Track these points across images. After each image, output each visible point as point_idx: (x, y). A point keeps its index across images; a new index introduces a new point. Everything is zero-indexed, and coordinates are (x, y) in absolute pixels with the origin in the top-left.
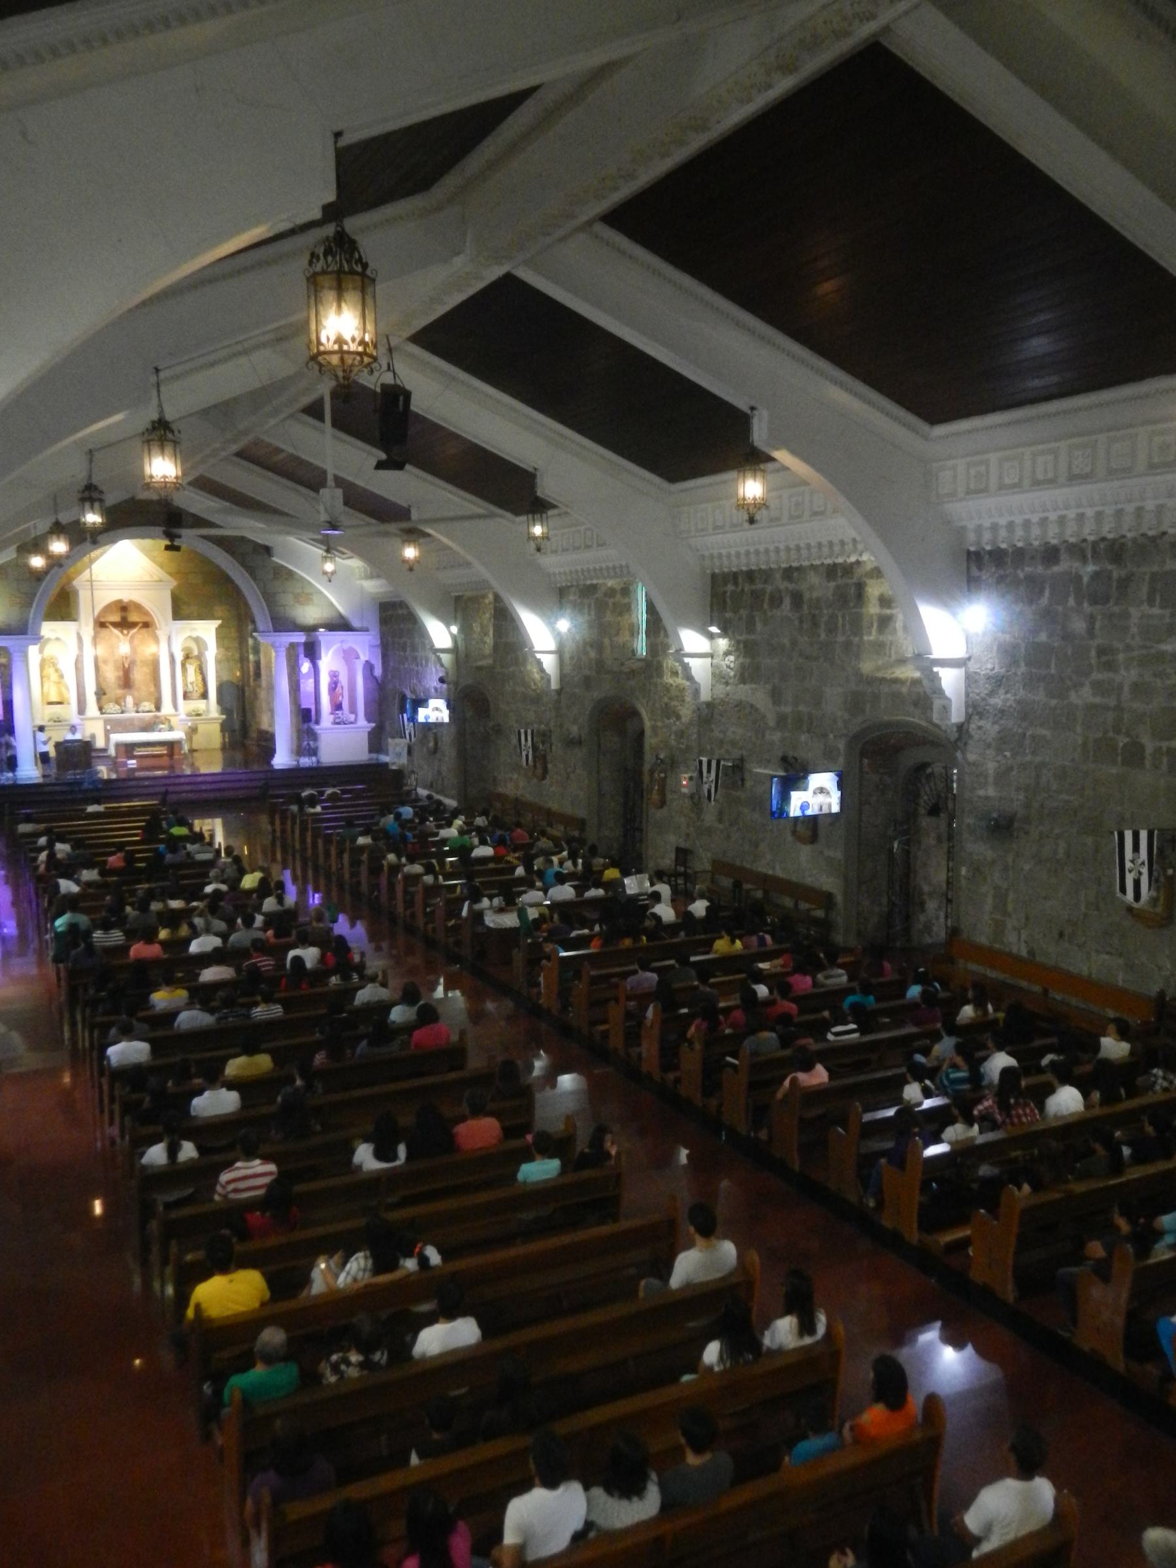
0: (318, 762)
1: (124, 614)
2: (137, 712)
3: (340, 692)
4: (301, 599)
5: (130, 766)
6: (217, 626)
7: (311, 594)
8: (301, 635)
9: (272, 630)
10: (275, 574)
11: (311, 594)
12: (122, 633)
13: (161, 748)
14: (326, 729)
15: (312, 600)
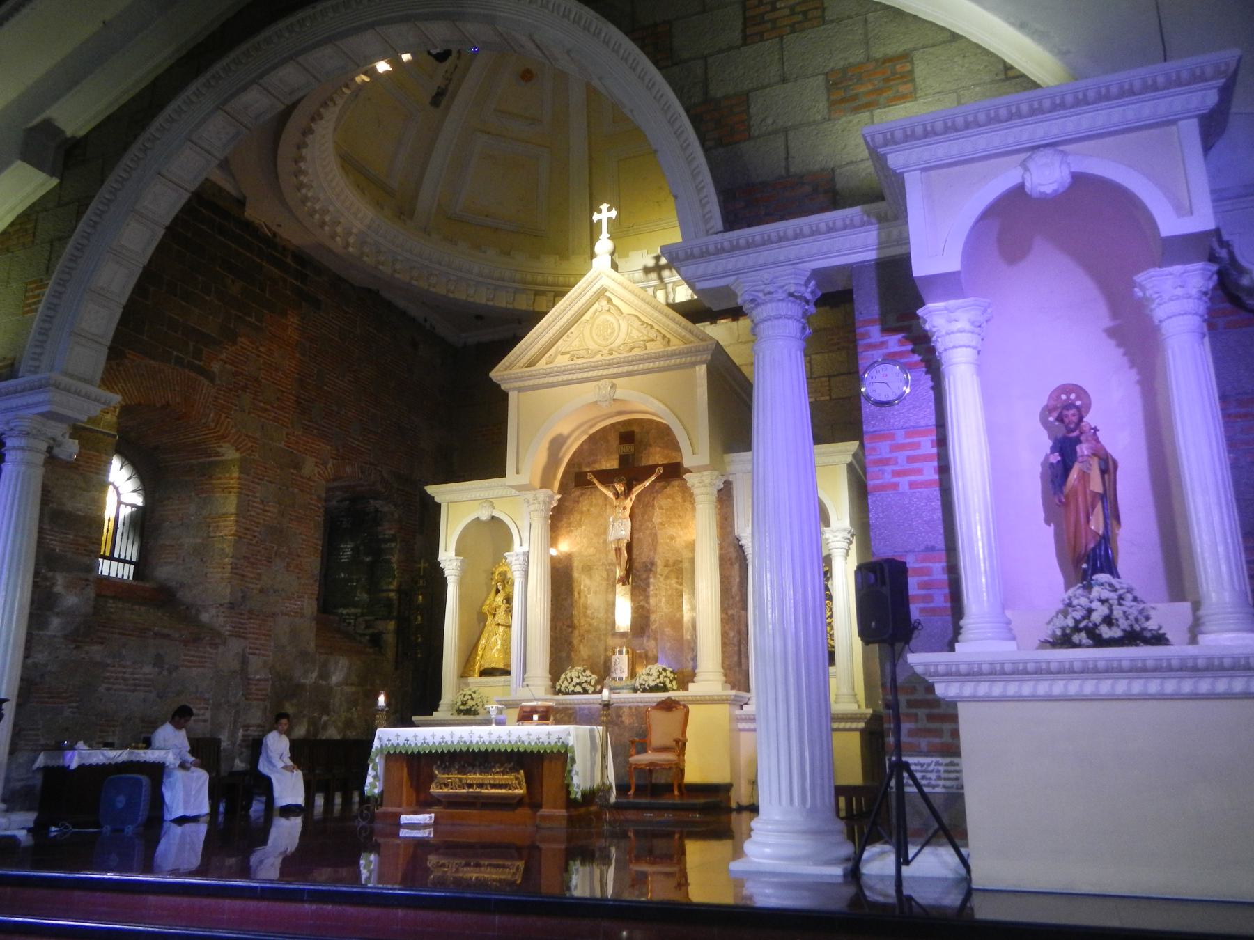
0: (965, 882)
1: (628, 449)
2: (635, 690)
3: (1096, 485)
4: (863, 89)
5: (404, 833)
6: (849, 458)
7: (906, 56)
8: (849, 226)
9: (718, 223)
10: (745, 19)
11: (906, 56)
12: (617, 495)
13: (509, 778)
14: (974, 673)
15: (908, 77)
